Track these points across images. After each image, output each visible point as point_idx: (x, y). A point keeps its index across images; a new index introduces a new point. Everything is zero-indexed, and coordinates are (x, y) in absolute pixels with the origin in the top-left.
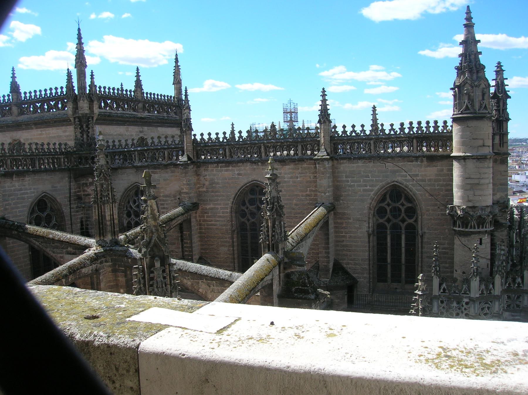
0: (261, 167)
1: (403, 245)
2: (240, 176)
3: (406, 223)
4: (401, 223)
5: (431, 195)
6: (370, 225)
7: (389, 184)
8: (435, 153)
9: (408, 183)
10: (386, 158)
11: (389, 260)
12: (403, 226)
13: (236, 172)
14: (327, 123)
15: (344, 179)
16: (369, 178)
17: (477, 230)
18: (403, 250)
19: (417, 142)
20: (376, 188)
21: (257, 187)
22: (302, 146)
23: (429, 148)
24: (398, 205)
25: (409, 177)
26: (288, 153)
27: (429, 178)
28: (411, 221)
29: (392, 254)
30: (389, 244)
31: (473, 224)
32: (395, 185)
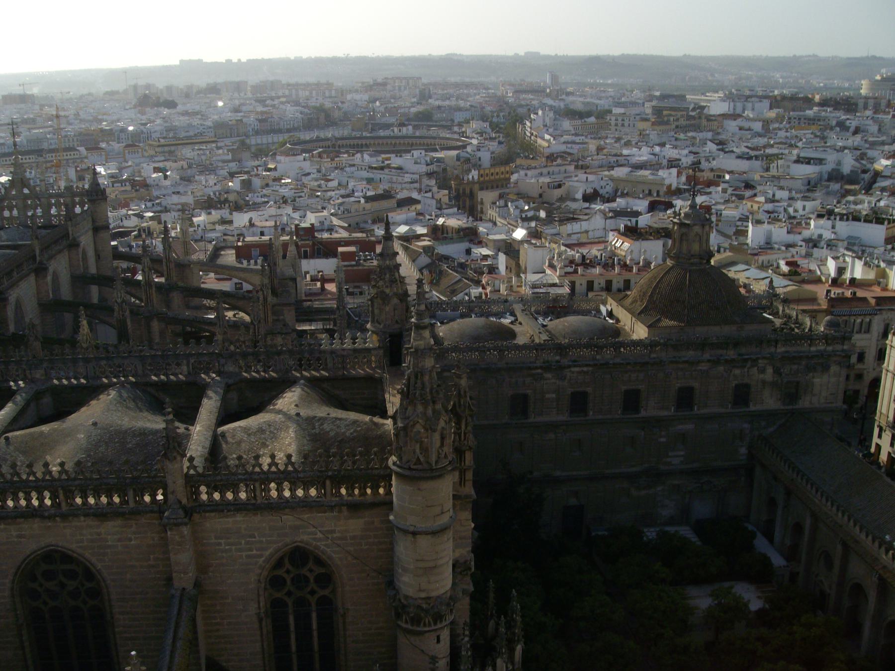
0: (62, 525)
1: (315, 626)
2: (23, 540)
3: (316, 596)
4: (309, 596)
5: (356, 558)
6: (261, 604)
7: (287, 545)
8: (361, 498)
9: (319, 544)
10: (281, 506)
11: (294, 648)
12: (313, 600)
13: (14, 534)
14: (179, 458)
15: (213, 541)
16: (255, 537)
17: (433, 627)
18: (315, 634)
19: (332, 483)
20: (268, 553)
21: (56, 551)
22: (134, 490)
23: (350, 492)
24: (305, 571)
25: (320, 535)
26: (110, 500)
27: (351, 534)
28: (326, 592)
29: (297, 639)
30: (292, 628)
31: (427, 621)
32: (298, 547)
